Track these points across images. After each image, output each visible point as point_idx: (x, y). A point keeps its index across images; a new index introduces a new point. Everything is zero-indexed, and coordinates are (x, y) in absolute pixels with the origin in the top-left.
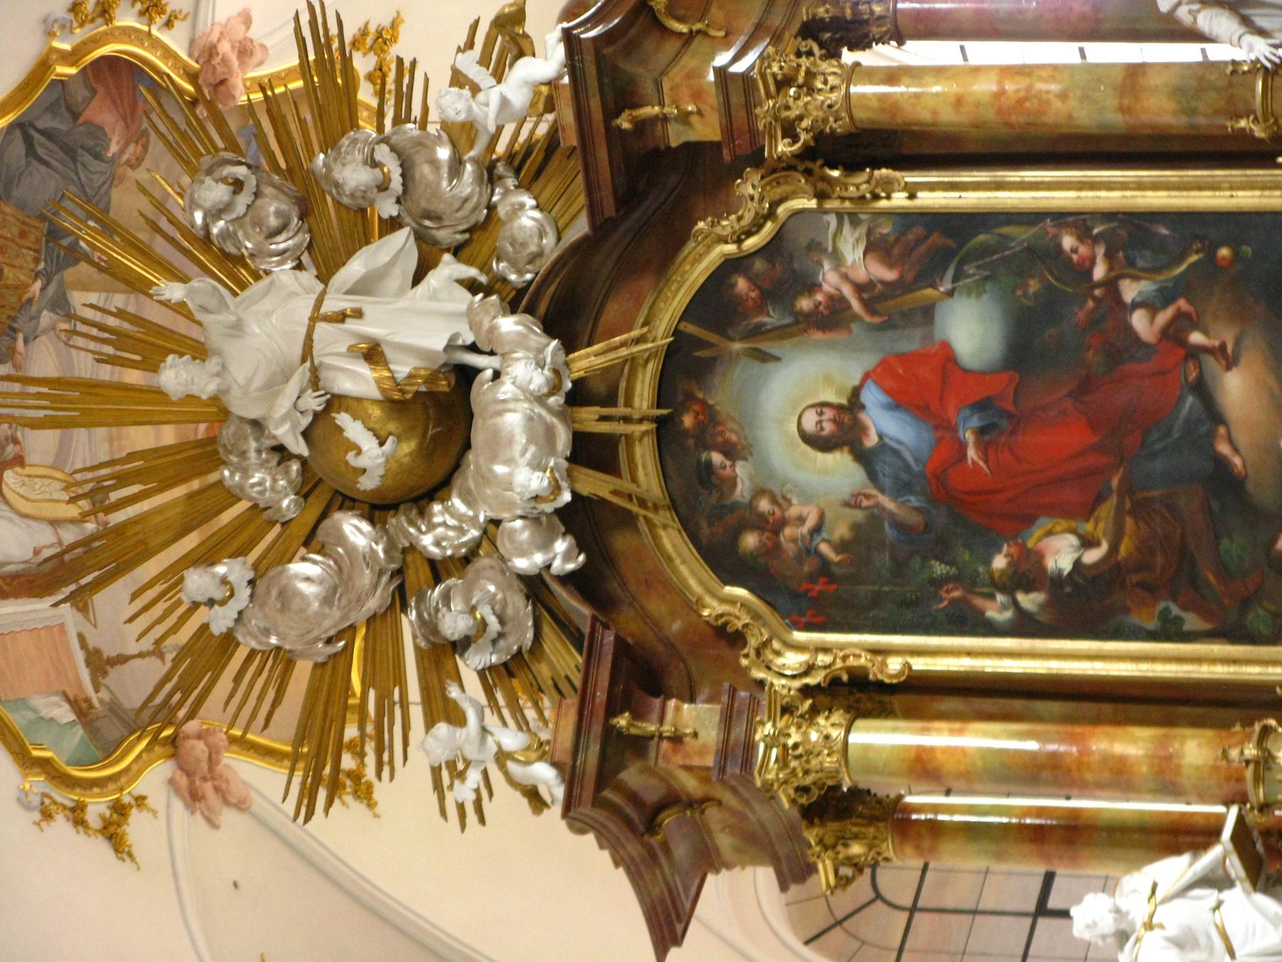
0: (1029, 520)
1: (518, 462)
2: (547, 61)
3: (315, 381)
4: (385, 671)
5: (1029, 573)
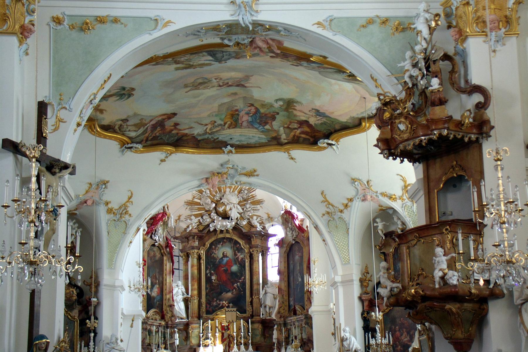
0: (217, 274)
1: (220, 224)
2: (259, 228)
3: (228, 204)
4: (199, 209)
5: (211, 274)
